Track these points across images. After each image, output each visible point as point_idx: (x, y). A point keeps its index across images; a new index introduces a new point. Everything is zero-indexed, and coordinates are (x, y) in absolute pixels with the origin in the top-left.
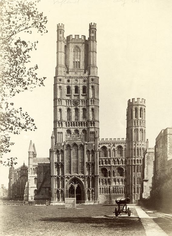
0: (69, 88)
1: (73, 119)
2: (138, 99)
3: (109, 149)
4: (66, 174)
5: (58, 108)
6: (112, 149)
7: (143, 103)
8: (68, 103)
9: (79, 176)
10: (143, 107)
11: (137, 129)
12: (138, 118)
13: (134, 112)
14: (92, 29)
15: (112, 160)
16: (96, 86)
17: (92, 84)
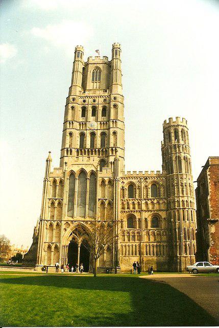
0: (84, 110)
1: (88, 145)
2: (177, 118)
3: (139, 186)
4: (66, 217)
5: (68, 131)
6: (143, 185)
7: (184, 124)
8: (83, 127)
9: (87, 222)
10: (186, 129)
11: (179, 157)
12: (178, 141)
13: (173, 135)
14: (115, 50)
15: (144, 202)
16: (120, 105)
17: (114, 103)
